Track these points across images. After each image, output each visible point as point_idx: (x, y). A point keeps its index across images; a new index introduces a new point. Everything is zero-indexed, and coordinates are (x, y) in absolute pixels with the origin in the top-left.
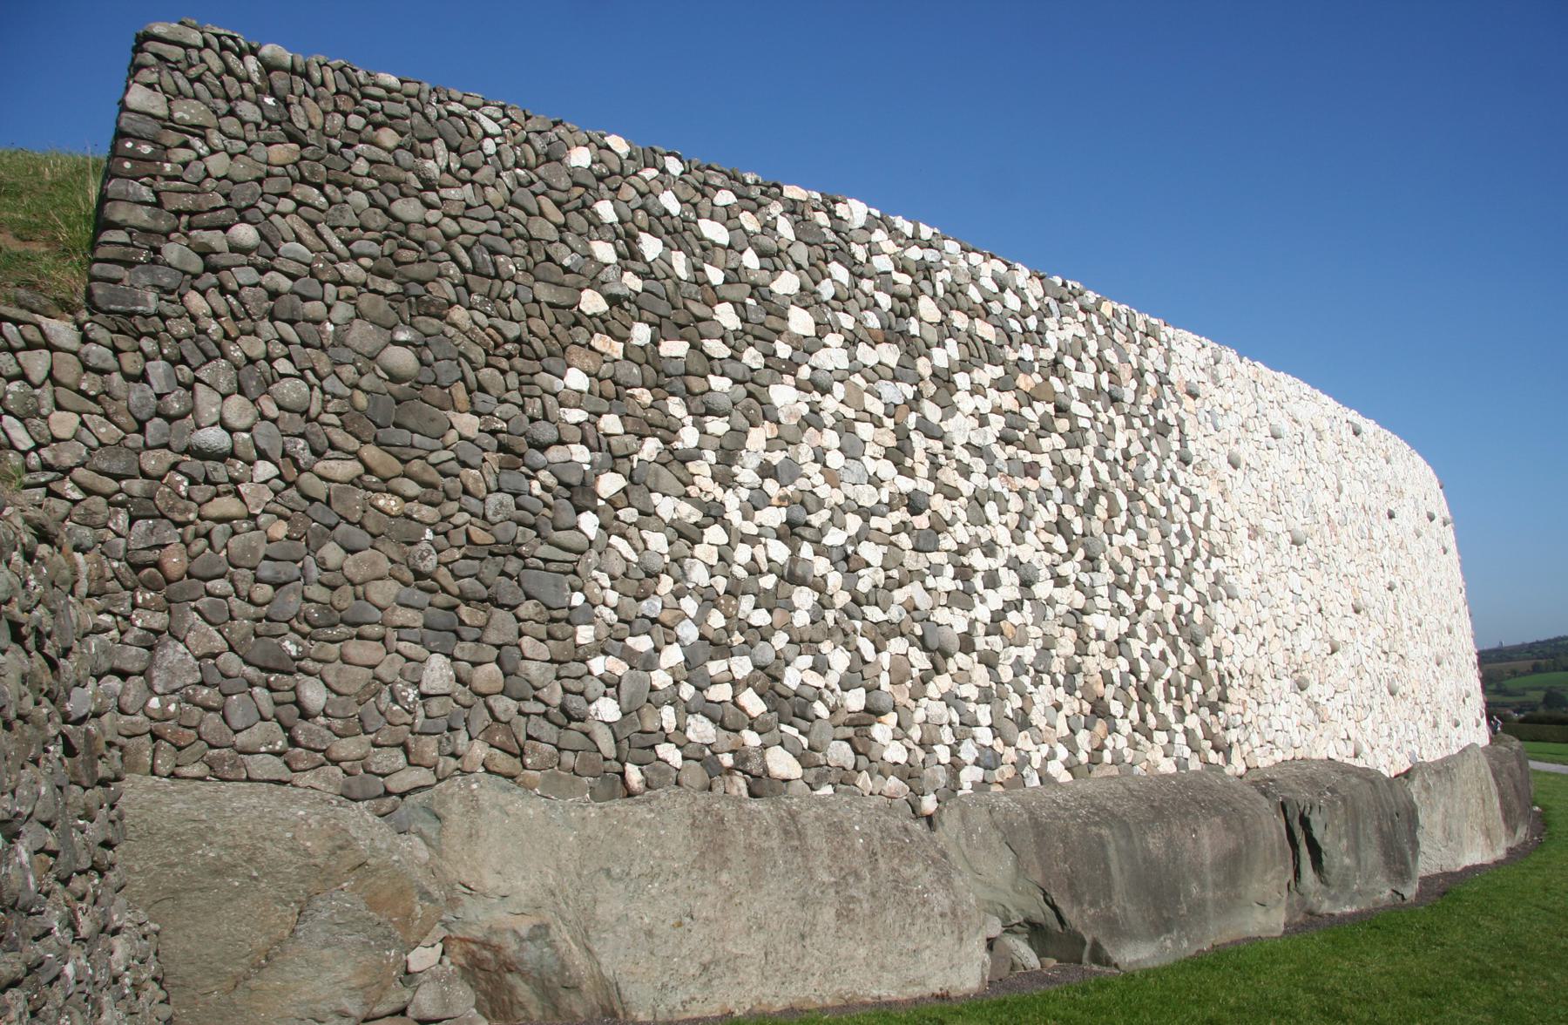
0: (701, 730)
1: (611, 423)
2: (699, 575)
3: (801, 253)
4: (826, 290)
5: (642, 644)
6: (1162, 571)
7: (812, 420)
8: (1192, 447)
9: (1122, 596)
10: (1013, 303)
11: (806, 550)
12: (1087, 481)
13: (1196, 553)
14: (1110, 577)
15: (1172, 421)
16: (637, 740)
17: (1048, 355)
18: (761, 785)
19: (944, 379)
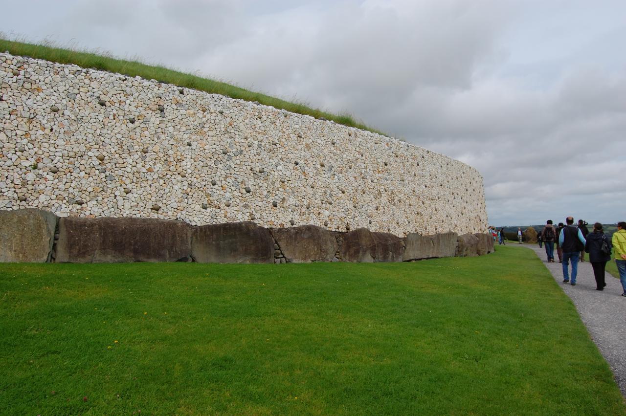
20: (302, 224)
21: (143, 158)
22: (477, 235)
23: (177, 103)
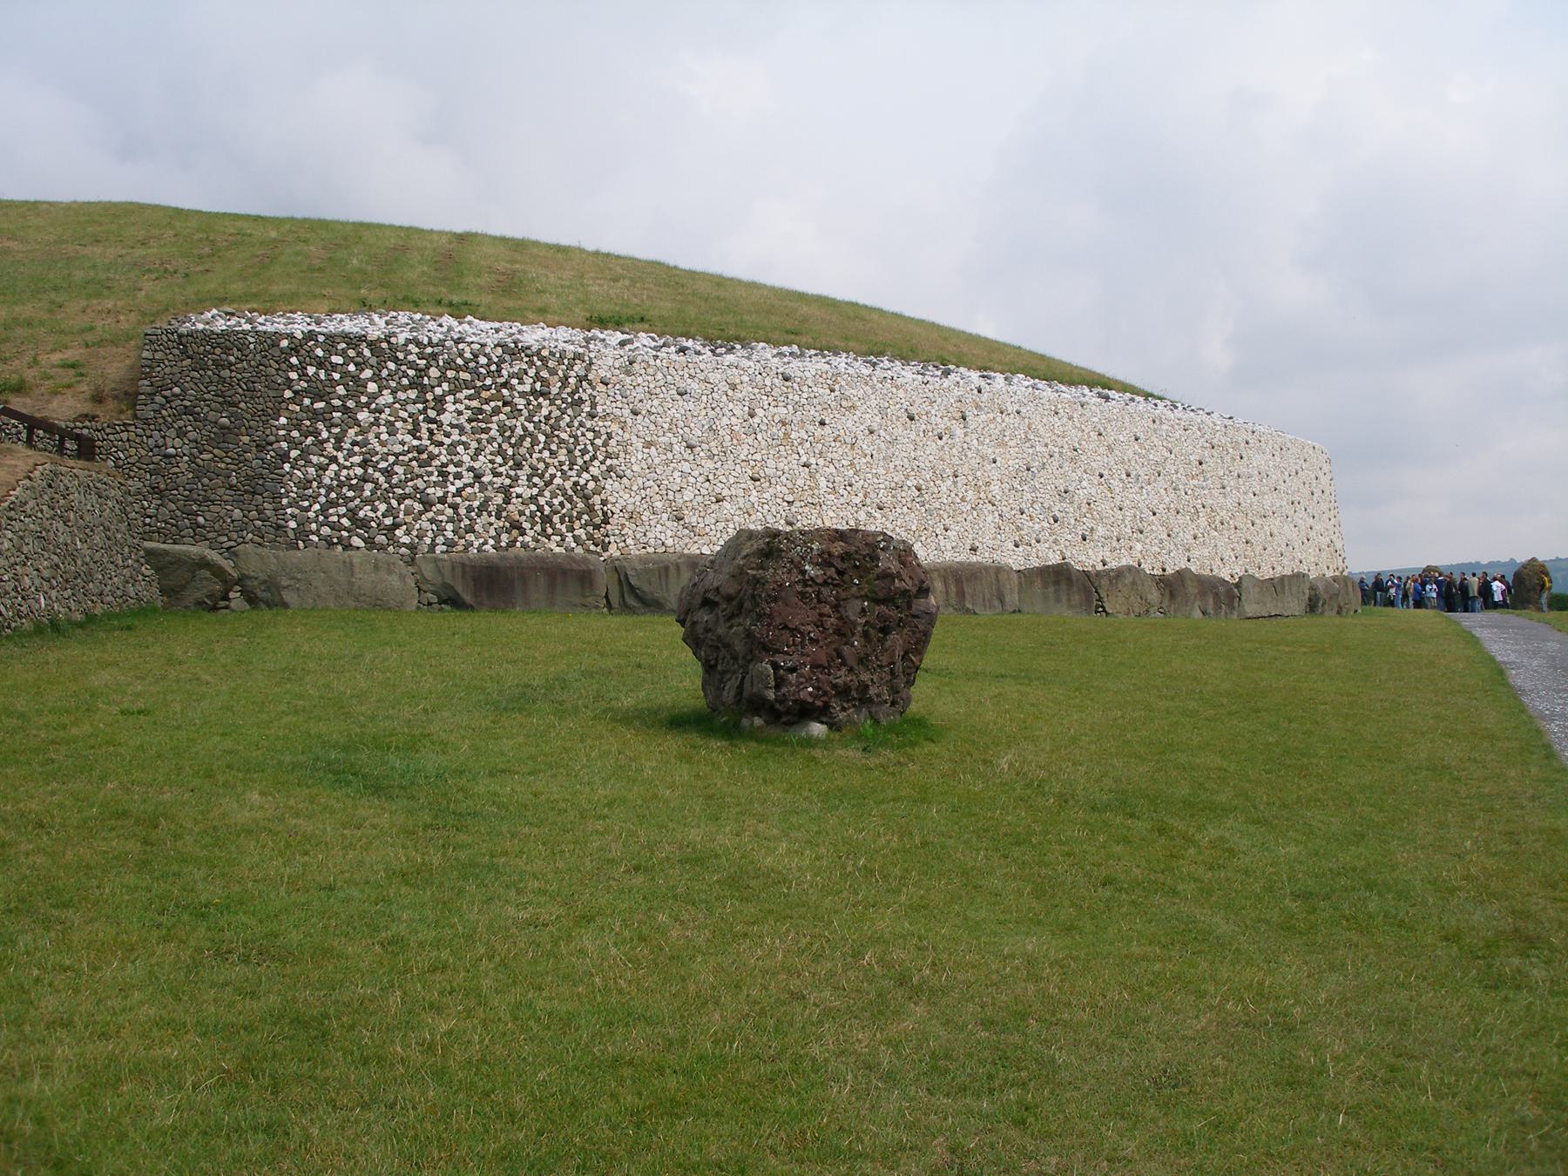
0: (326, 530)
1: (295, 434)
2: (327, 481)
3: (373, 361)
4: (385, 373)
5: (306, 504)
6: (565, 468)
7: (376, 423)
8: (599, 409)
9: (536, 480)
10: (483, 360)
11: (370, 470)
12: (519, 431)
13: (594, 458)
14: (529, 471)
15: (585, 397)
16: (302, 533)
17: (502, 380)
18: (349, 547)
19: (440, 400)
20: (1113, 565)
21: (955, 483)
22: (1335, 579)
23: (978, 407)
